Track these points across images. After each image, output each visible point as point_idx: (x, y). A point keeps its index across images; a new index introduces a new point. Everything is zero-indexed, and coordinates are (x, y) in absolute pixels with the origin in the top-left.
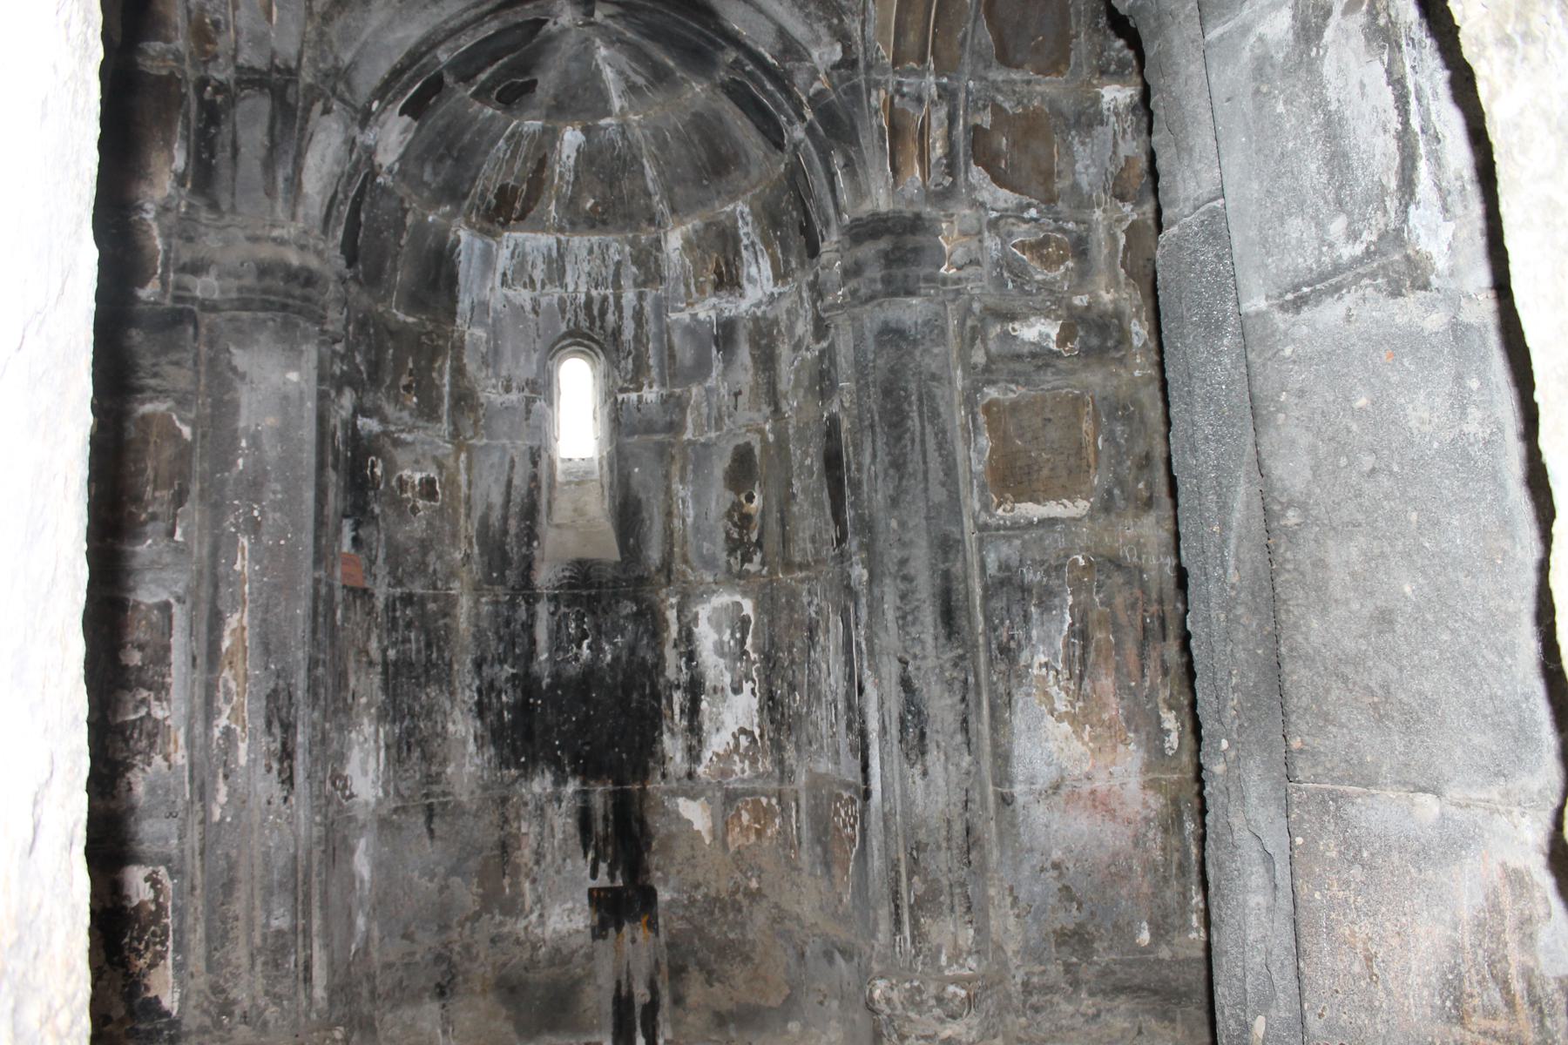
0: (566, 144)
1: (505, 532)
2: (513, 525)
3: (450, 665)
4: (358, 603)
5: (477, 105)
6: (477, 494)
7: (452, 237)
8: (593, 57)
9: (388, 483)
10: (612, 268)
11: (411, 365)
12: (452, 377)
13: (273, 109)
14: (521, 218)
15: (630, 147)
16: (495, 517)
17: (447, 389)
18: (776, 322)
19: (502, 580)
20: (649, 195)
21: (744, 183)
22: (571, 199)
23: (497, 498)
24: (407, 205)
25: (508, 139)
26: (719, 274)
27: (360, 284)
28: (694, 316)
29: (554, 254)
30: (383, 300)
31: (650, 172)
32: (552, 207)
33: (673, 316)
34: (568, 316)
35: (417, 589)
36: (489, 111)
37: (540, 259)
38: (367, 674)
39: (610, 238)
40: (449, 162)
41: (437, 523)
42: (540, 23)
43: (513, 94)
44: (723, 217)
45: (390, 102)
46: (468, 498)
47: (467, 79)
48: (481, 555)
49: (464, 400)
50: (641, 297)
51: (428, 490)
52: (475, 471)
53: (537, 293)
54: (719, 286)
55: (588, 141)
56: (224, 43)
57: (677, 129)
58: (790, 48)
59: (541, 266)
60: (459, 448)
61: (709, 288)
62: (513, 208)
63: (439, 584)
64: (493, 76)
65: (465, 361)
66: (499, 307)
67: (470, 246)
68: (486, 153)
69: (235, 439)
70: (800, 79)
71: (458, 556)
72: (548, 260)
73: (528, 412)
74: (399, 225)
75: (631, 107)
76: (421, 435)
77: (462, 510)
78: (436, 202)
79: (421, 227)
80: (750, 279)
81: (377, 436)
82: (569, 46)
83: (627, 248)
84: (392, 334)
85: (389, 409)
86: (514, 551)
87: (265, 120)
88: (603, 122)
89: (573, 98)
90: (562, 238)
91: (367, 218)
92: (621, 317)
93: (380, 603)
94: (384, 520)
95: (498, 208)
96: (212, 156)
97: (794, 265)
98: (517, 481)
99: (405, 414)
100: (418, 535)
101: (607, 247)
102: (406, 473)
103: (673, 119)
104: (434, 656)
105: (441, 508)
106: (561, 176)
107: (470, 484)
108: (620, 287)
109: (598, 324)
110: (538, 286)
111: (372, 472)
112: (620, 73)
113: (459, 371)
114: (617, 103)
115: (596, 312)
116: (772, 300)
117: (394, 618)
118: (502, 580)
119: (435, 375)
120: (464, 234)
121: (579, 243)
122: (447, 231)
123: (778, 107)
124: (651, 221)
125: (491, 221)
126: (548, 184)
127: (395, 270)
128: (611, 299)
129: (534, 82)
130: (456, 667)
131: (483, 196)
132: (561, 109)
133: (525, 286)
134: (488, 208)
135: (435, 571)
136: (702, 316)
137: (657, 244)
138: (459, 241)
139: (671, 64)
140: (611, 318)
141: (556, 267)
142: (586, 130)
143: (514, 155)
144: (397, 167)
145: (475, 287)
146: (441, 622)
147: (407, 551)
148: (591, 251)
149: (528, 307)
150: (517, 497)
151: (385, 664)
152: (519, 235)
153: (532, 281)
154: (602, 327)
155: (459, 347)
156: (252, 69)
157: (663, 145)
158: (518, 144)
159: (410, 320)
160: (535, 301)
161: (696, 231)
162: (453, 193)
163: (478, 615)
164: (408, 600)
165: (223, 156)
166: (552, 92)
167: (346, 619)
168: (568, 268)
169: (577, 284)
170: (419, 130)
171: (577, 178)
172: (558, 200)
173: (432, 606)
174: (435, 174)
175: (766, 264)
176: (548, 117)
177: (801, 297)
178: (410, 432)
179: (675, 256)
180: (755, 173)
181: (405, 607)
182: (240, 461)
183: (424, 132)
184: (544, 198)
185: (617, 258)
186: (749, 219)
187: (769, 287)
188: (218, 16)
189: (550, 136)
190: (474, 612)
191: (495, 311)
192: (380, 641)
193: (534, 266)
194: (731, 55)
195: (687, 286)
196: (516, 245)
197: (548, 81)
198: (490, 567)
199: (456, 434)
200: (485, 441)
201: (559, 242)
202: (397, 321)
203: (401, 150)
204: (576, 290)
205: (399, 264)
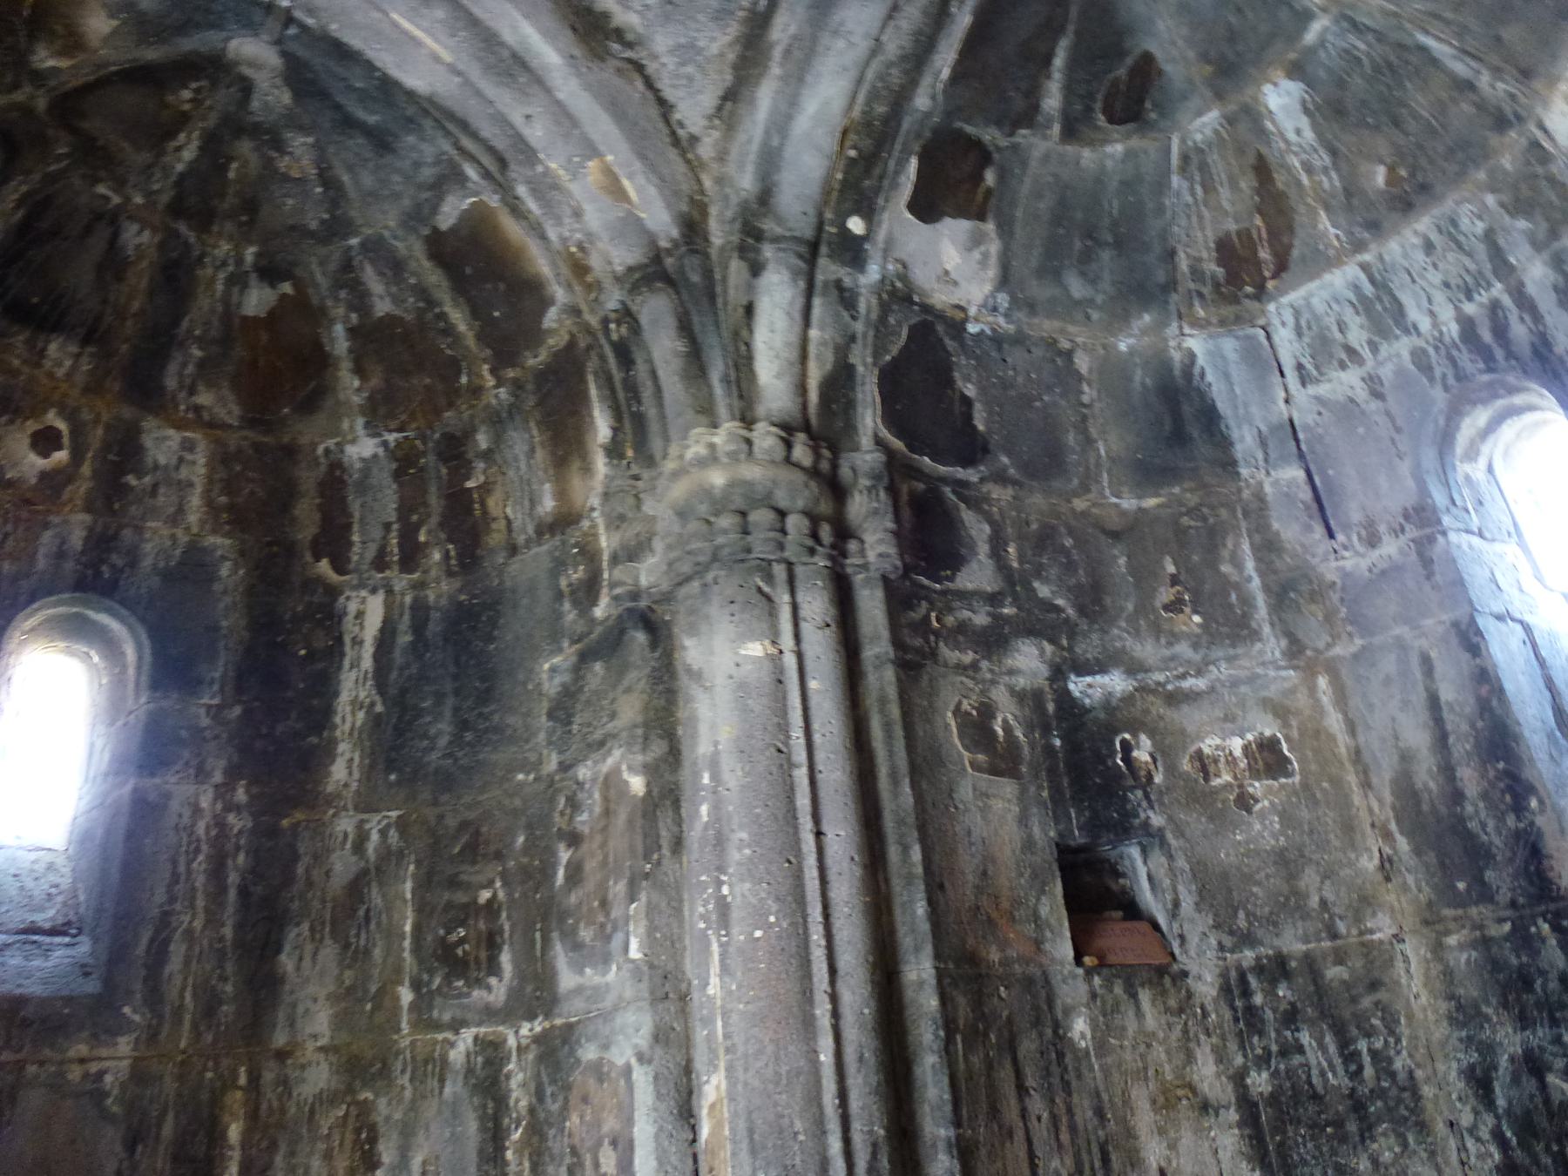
0: (1280, 116)
1: (1457, 796)
2: (1470, 779)
3: (1413, 1087)
4: (1145, 996)
6: (1372, 740)
7: (1176, 356)
9: (1171, 770)
10: (1481, 250)
11: (1171, 569)
12: (1258, 560)
13: (682, 303)
14: (1281, 267)
15: (1380, 37)
16: (1425, 774)
17: (1256, 582)
19: (1485, 895)
20: (1467, 86)
22: (1348, 193)
23: (1418, 737)
24: (1065, 345)
25: (1184, 169)
27: (1015, 483)
29: (1368, 289)
30: (1085, 489)
34: (1438, 372)
35: (1292, 942)
36: (1118, 149)
37: (1349, 311)
38: (1199, 1131)
39: (1448, 205)
40: (1106, 255)
41: (1305, 814)
46: (1357, 754)
48: (1417, 851)
49: (1291, 590)
51: (1268, 759)
52: (1355, 702)
55: (1310, 83)
56: (595, 261)
60: (1310, 672)
62: (1258, 264)
63: (1342, 927)
64: (1069, 90)
65: (1276, 525)
66: (1310, 419)
67: (1217, 355)
68: (1160, 210)
69: (697, 775)
71: (1369, 864)
72: (1364, 305)
73: (1427, 562)
74: (1067, 377)
76: (1222, 671)
77: (1352, 779)
81: (1128, 699)
83: (1490, 200)
84: (1115, 535)
85: (1146, 650)
86: (1492, 832)
87: (670, 322)
88: (1311, 36)
89: (1232, 37)
91: (983, 390)
92: (1537, 317)
93: (1206, 986)
94: (1180, 833)
95: (1234, 279)
96: (639, 402)
98: (1447, 694)
99: (1183, 649)
100: (1269, 843)
101: (1454, 222)
102: (1208, 745)
104: (1369, 1072)
105: (1305, 786)
106: (1309, 168)
107: (1352, 729)
108: (1512, 268)
109: (1499, 354)
110: (1366, 353)
111: (1127, 759)
113: (1268, 547)
115: (1487, 336)
117: (1250, 1010)
118: (1485, 895)
119: (1225, 568)
120: (1196, 343)
121: (1402, 246)
122: (1166, 349)
124: (1501, 122)
125: (1235, 300)
126: (1292, 193)
127: (1089, 442)
128: (1507, 301)
129: (1147, 59)
130: (1427, 1091)
131: (1197, 273)
132: (1229, 69)
133: (1343, 366)
134: (1217, 285)
135: (1323, 903)
138: (1192, 356)
140: (1520, 331)
141: (1382, 308)
142: (1296, 71)
143: (1209, 187)
144: (1003, 300)
145: (1254, 409)
146: (1366, 1002)
147: (1249, 879)
148: (1429, 247)
149: (1361, 393)
150: (1458, 725)
151: (1246, 1102)
152: (1294, 296)
153: (1351, 351)
154: (1510, 355)
155: (1257, 511)
156: (631, 269)
158: (1204, 167)
159: (1151, 502)
160: (1372, 382)
163: (1448, 974)
164: (1277, 969)
165: (647, 393)
166: (1191, 54)
167: (1104, 1032)
169: (1433, 313)
170: (1005, 230)
171: (1334, 153)
172: (1328, 208)
173: (1334, 973)
174: (1093, 281)
176: (1220, 96)
178: (1199, 673)
181: (1274, 983)
182: (704, 809)
183: (1019, 232)
184: (1301, 218)
185: (1480, 227)
188: (578, 236)
189: (1251, 117)
190: (1436, 969)
192: (1221, 1057)
196: (1297, 313)
198: (1445, 870)
199: (1295, 649)
200: (1359, 642)
201: (1365, 267)
202: (1124, 514)
203: (992, 272)
204: (1435, 325)
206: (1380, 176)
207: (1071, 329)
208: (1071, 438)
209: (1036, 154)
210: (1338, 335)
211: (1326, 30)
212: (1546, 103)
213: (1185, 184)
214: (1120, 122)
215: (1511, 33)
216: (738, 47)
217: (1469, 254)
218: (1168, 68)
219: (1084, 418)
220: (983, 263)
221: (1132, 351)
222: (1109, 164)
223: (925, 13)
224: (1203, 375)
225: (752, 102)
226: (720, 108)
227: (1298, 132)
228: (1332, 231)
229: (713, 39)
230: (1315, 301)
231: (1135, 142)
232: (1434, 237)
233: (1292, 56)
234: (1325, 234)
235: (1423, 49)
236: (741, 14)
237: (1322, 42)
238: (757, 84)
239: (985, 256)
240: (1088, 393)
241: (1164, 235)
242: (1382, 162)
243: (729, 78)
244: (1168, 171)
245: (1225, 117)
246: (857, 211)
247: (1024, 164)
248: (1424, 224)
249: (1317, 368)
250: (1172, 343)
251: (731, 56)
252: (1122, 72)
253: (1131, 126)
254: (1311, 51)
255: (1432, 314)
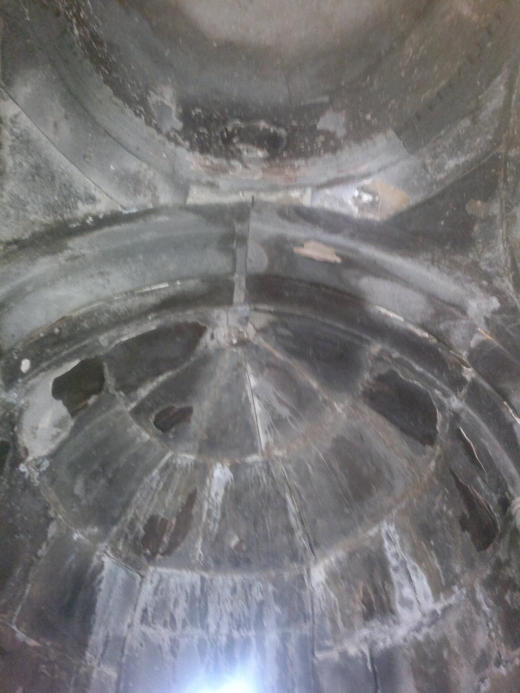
0: (215, 482)
5: (135, 427)
7: (95, 561)
8: (243, 388)
14: (168, 552)
15: (274, 483)
18: (444, 642)
21: (388, 501)
24: (51, 513)
26: (368, 604)
28: (344, 654)
29: (198, 592)
31: (292, 508)
32: (199, 545)
33: (320, 656)
36: (146, 436)
39: (252, 577)
42: (199, 331)
43: (170, 421)
44: (367, 543)
45: (44, 370)
47: (128, 388)
50: (284, 638)
53: (178, 633)
54: (369, 615)
55: (236, 478)
57: (318, 459)
58: (445, 310)
59: (183, 604)
61: (357, 620)
62: (160, 541)
64: (153, 394)
66: (136, 644)
67: (113, 575)
68: (140, 480)
70: (457, 337)
72: (192, 599)
74: (39, 533)
75: (276, 442)
78: (83, 521)
79: (63, 544)
80: (407, 603)
82: (221, 372)
83: (271, 588)
89: (224, 433)
90: (206, 576)
95: (146, 541)
97: (457, 569)
101: (250, 586)
103: (315, 449)
110: (179, 624)
112: (267, 406)
114: (263, 439)
116: (435, 618)
120: (108, 562)
121: (224, 581)
122: (92, 554)
123: (432, 384)
124: (294, 557)
125: (138, 552)
127: (25, 580)
131: (132, 525)
132: (213, 444)
133: (165, 625)
134: (136, 538)
136: (352, 651)
137: (301, 581)
138: (102, 566)
139: (315, 384)
142: (235, 468)
143: (166, 488)
144: (46, 464)
145: (112, 620)
148: (234, 591)
149: (166, 646)
152: (164, 571)
153: (173, 619)
157: (305, 478)
158: (171, 477)
159: (32, 643)
160: (174, 642)
161: (339, 562)
162: (103, 514)
166: (205, 424)
168: (211, 609)
171: (223, 515)
172: (205, 538)
174: (87, 490)
175: (422, 583)
176: (200, 452)
177: (476, 604)
179: (319, 592)
180: (399, 485)
184: (191, 534)
185: (260, 597)
186: (397, 537)
187: (430, 605)
189: (203, 471)
191: (131, 648)
193: (176, 603)
194: (376, 348)
195: (333, 621)
196: (161, 580)
197: (203, 410)
202: (14, 640)
203: (52, 446)
204: (217, 632)
205: (31, 575)
206: (234, 542)
207: (61, 508)
208: (18, 571)
209: (118, 408)
210: (171, 606)
211: (257, 462)
212: (316, 563)
213: (158, 477)
214: (157, 426)
215: (320, 523)
216: (43, 229)
217: (249, 607)
218: (193, 423)
219: (32, 563)
220: (55, 437)
221: (78, 543)
222: (138, 440)
223: (140, 306)
224: (100, 582)
225: (33, 260)
226: (9, 244)
227: (217, 494)
228: (200, 551)
229: (36, 213)
230: (172, 580)
231: (155, 440)
232: (239, 587)
233: (238, 461)
234: (195, 550)
235: (285, 501)
236: (59, 218)
237: (252, 466)
238: (45, 254)
239: (58, 434)
240: (43, 551)
241: (132, 494)
242: (239, 536)
243: (27, 236)
244: (154, 466)
245: (195, 462)
246: (32, 359)
247: (109, 407)
248: (238, 578)
249: (153, 617)
250: (98, 553)
251: (37, 229)
252: (177, 406)
253: (160, 432)
254: (247, 465)
255: (218, 625)
